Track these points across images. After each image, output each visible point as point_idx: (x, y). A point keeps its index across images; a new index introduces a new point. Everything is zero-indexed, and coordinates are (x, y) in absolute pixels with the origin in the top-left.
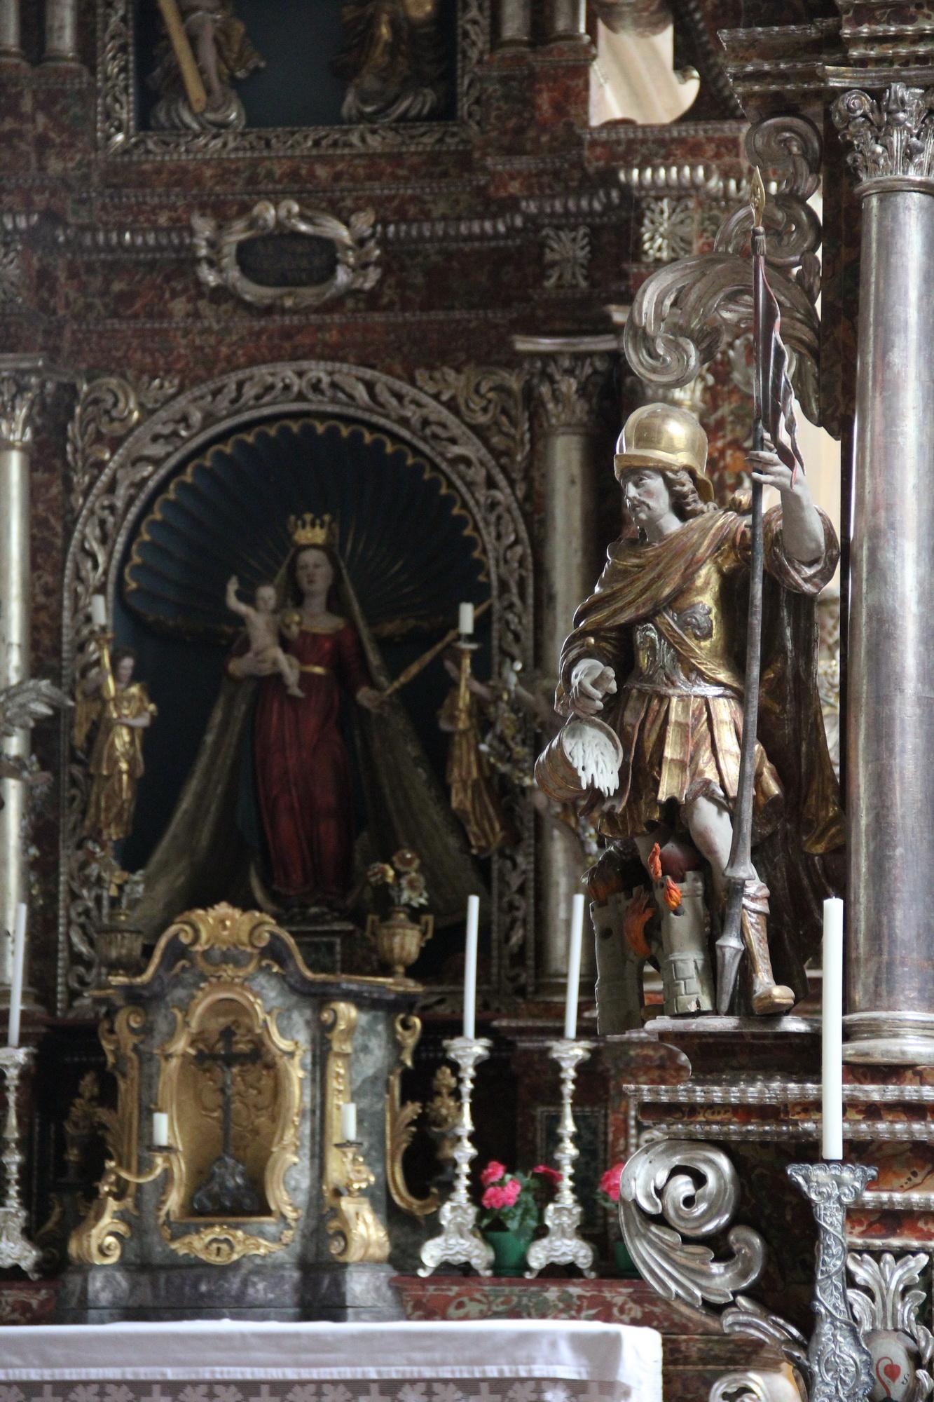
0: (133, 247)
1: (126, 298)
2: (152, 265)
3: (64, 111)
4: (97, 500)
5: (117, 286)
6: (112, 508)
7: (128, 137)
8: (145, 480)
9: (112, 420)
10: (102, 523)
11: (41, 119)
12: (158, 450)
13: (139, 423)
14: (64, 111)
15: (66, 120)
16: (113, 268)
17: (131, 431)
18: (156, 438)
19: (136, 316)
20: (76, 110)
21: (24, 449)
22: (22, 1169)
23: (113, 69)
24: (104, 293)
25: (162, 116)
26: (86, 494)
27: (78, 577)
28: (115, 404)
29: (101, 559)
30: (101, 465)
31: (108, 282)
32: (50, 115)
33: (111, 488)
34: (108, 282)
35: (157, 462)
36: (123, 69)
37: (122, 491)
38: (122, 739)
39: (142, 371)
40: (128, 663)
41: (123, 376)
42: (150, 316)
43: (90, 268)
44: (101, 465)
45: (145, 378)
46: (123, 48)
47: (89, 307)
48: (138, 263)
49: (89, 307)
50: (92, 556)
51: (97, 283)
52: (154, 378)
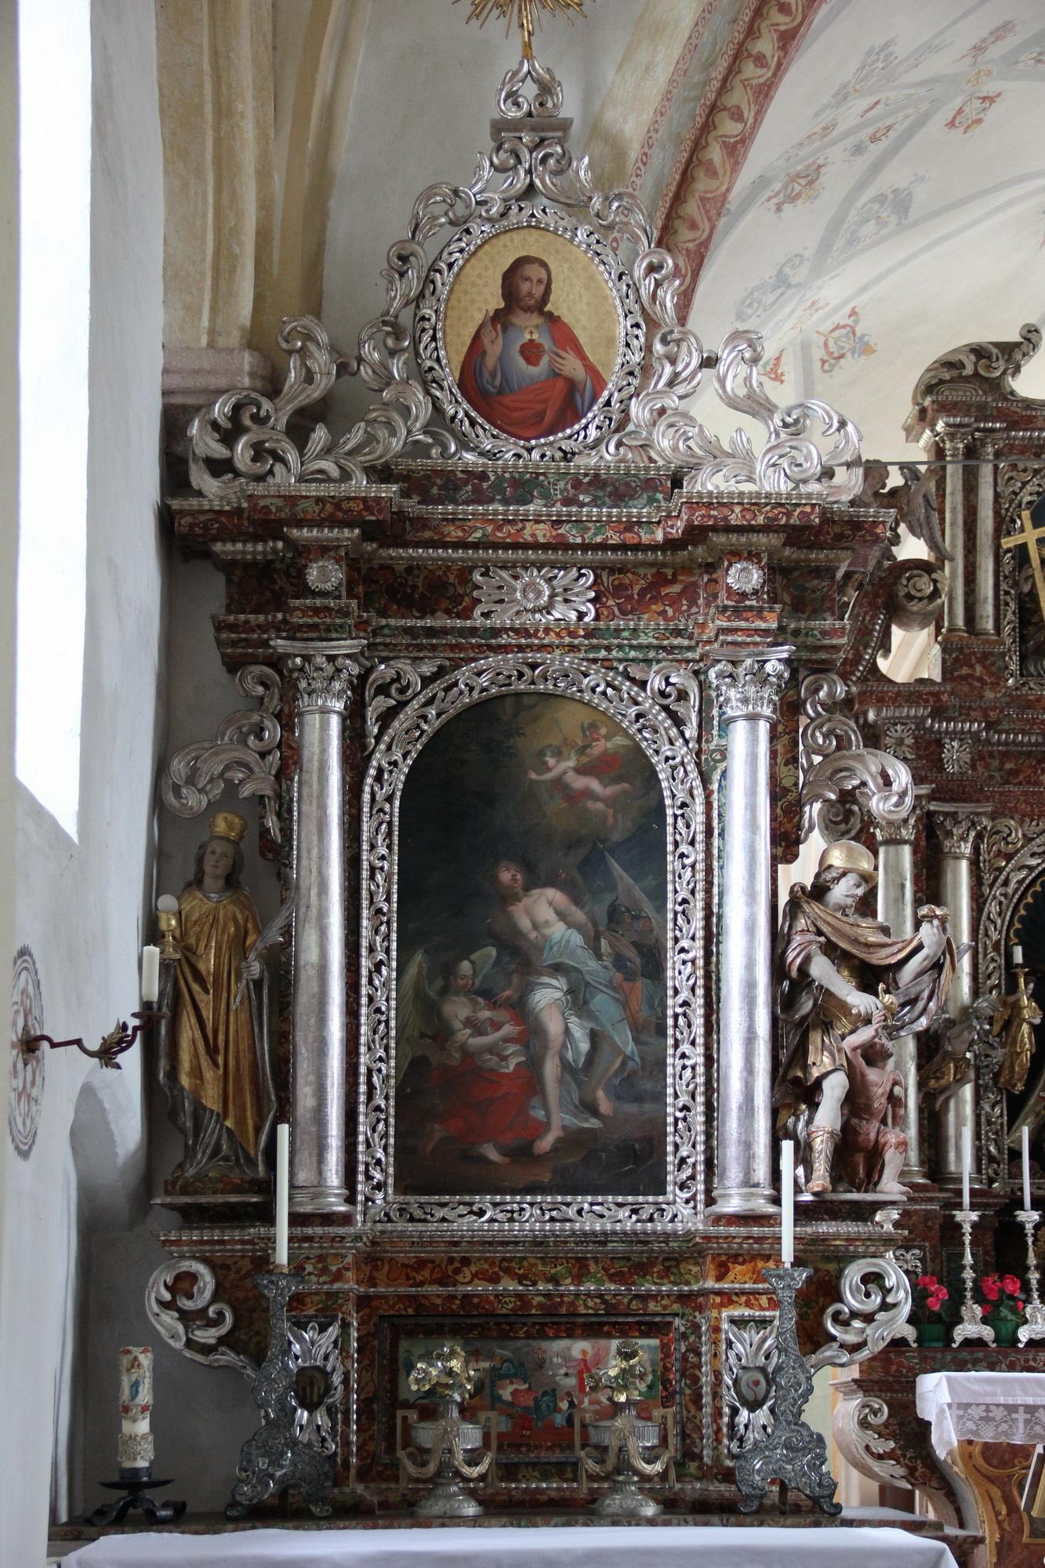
0: (1021, 743)
1: (1014, 773)
2: (1029, 754)
3: (993, 664)
4: (998, 891)
5: (1008, 766)
6: (1005, 895)
7: (1017, 681)
8: (1024, 879)
9: (1008, 843)
10: (1001, 903)
11: (979, 668)
12: (1033, 862)
13: (1023, 847)
14: (993, 664)
15: (993, 669)
16: (1005, 756)
17: (1018, 851)
18: (1033, 855)
19: (1020, 783)
20: (1000, 663)
21: (969, 859)
22: (1039, 1282)
23: (1009, 641)
24: (1001, 769)
25: (1032, 669)
26: (991, 886)
27: (986, 935)
28: (1009, 835)
29: (999, 922)
30: (1000, 870)
31: (1002, 763)
32: (984, 667)
33: (1006, 883)
34: (1002, 763)
35: (1031, 868)
36: (1014, 642)
37: (1013, 885)
38: (1025, 1028)
39: (1024, 816)
40: (1031, 986)
41: (1012, 818)
42: (1028, 783)
43: (991, 755)
44: (1000, 870)
45: (1028, 820)
46: (1014, 629)
47: (991, 777)
48: (1020, 753)
49: (991, 777)
50: (994, 922)
51: (996, 763)
52: (1032, 820)
